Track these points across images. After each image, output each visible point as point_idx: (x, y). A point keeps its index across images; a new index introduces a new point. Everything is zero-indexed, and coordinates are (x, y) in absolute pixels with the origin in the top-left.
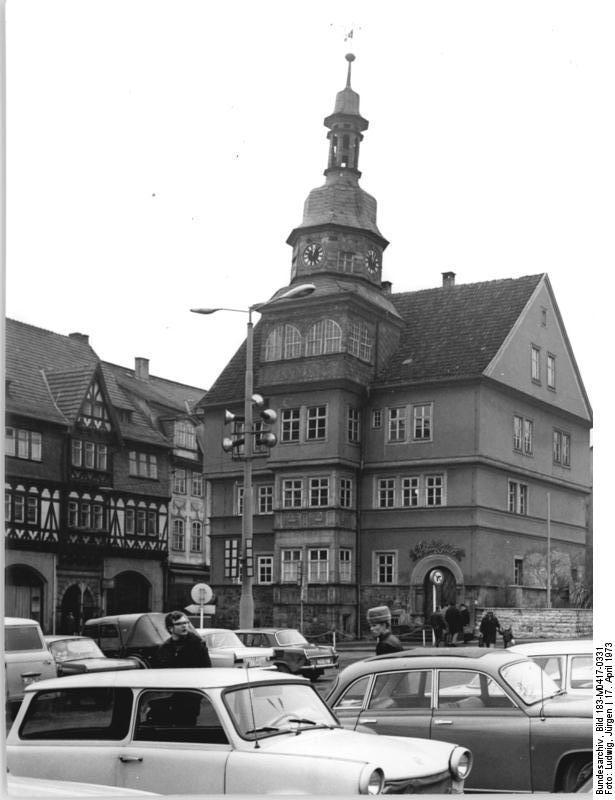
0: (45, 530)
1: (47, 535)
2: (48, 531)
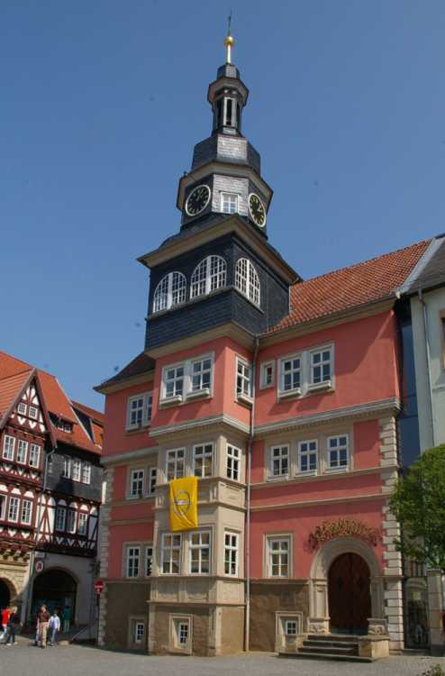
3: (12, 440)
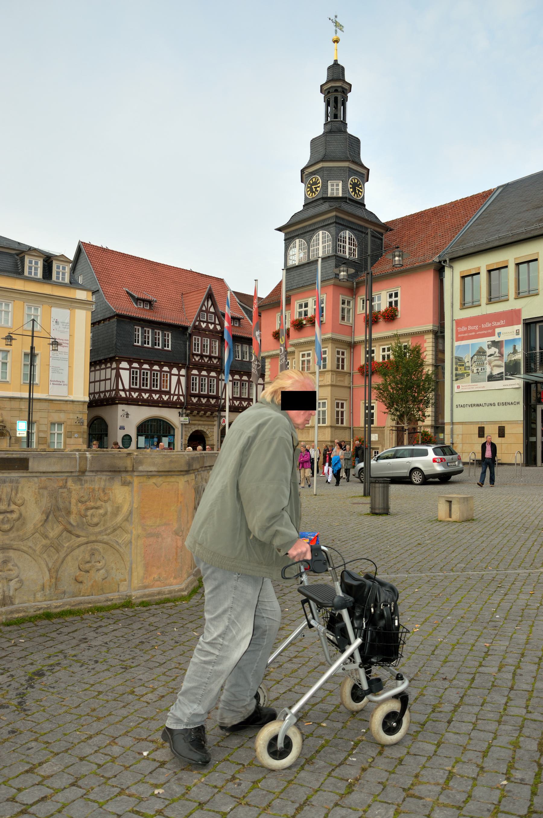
0: (174, 395)
1: (176, 397)
2: (176, 395)
3: (198, 339)
